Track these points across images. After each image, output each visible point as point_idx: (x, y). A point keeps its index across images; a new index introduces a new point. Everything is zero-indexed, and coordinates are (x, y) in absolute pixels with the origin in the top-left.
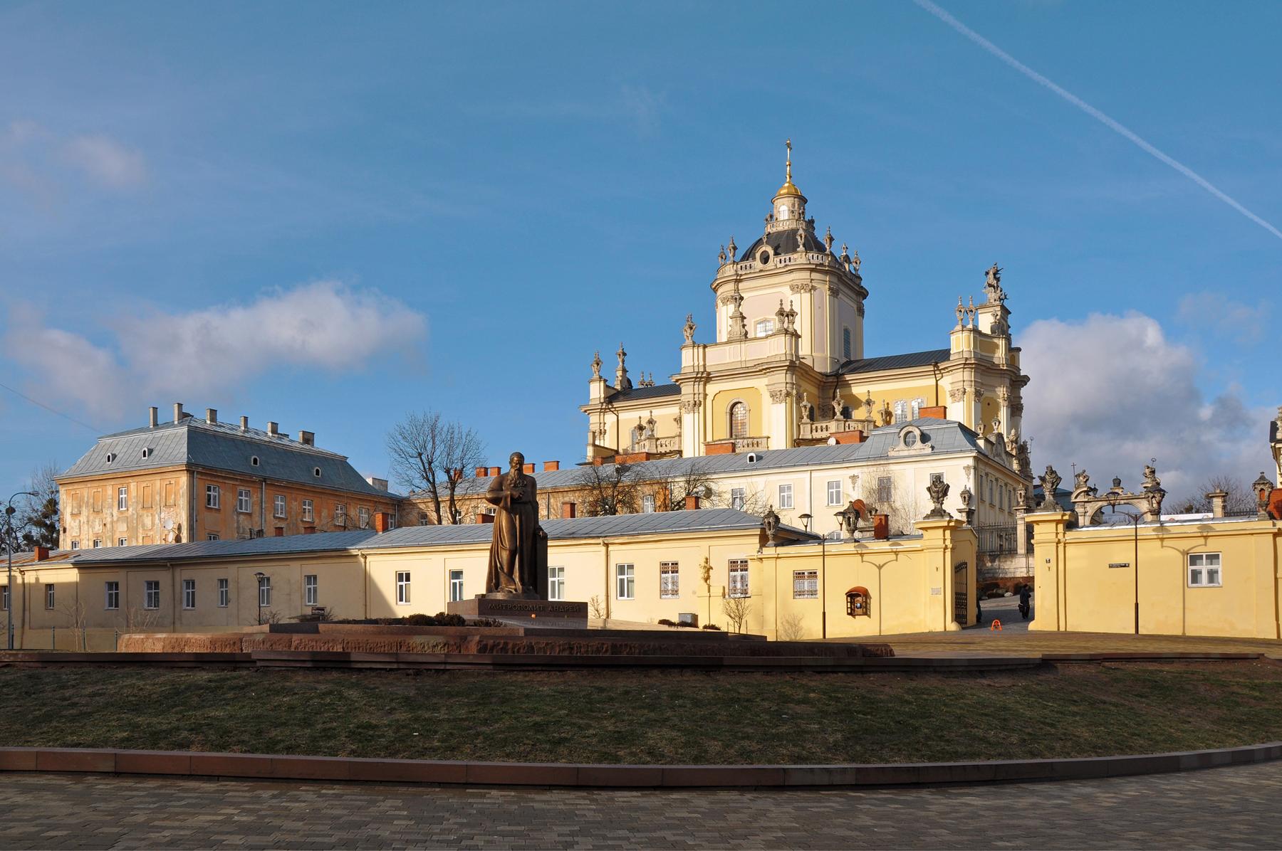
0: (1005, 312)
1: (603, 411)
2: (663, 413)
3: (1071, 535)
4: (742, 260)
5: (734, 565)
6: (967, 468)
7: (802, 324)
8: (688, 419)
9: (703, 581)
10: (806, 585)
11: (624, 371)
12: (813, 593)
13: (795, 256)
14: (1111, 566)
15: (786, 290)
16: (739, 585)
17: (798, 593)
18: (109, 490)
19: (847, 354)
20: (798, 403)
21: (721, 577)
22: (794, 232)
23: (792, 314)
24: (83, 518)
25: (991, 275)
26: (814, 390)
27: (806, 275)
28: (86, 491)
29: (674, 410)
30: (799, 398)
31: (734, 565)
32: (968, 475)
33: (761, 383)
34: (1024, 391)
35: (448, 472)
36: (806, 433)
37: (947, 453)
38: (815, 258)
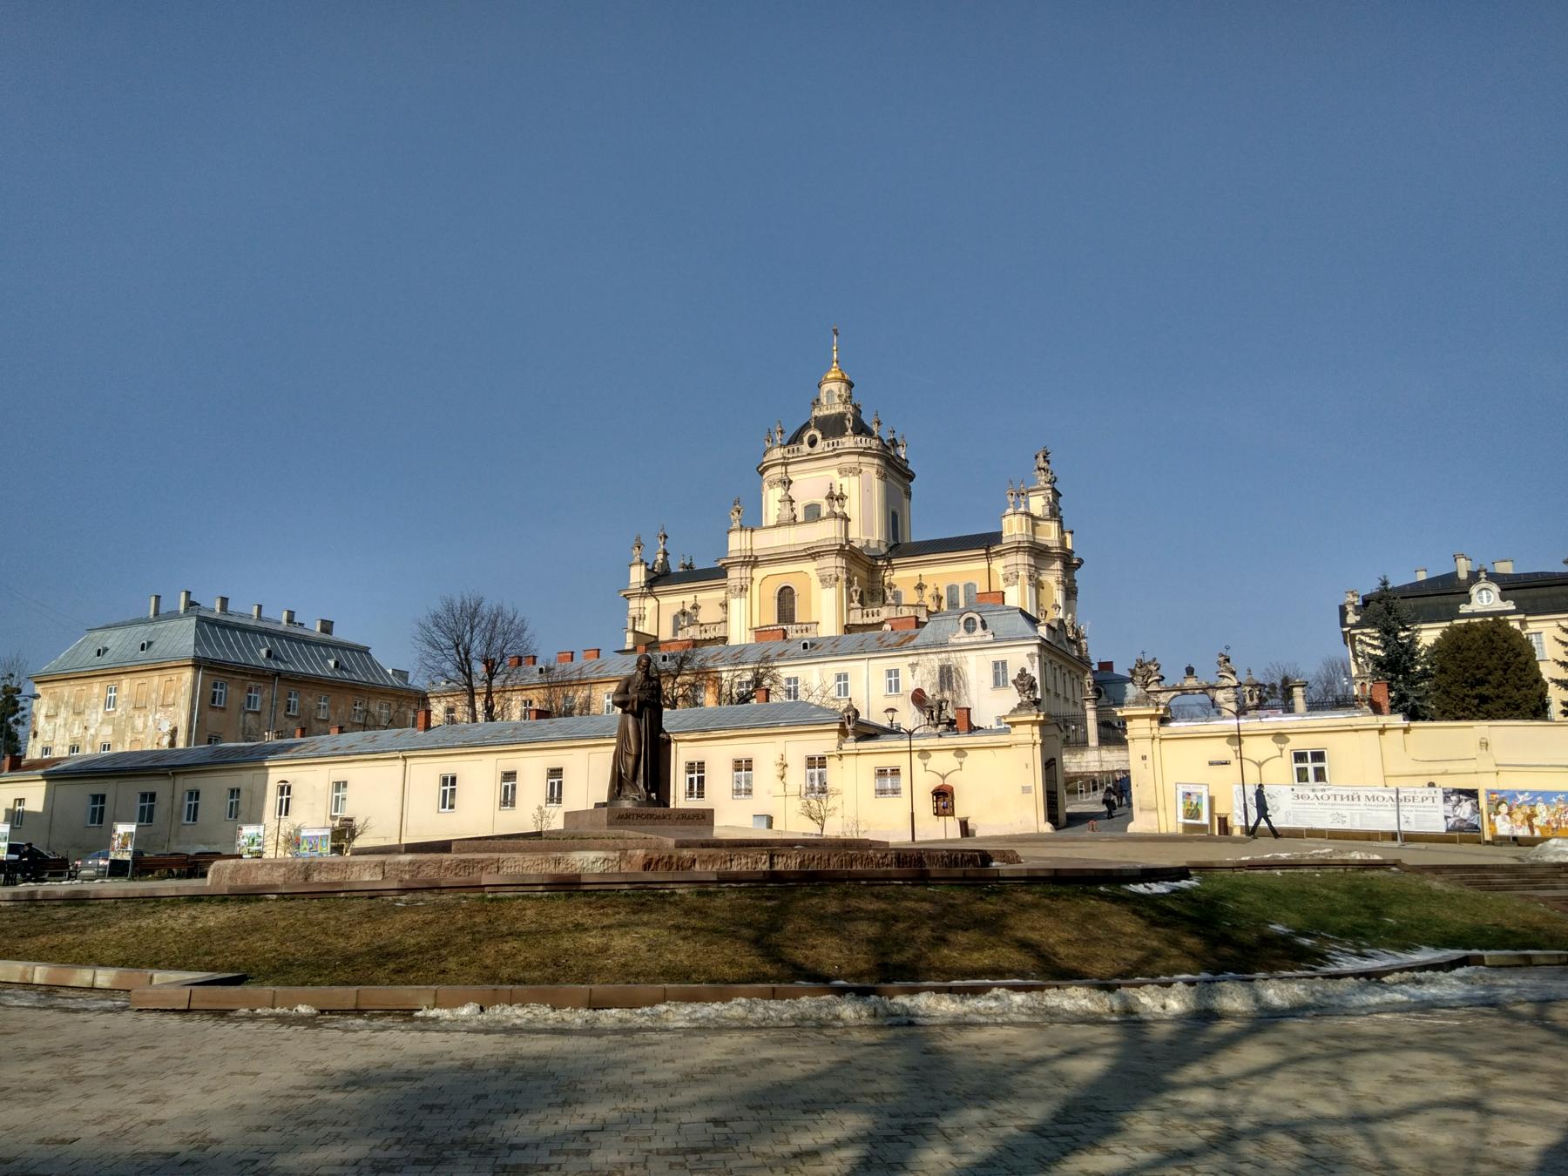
0: (1057, 494)
1: (643, 596)
2: (708, 600)
3: (1164, 730)
4: (789, 443)
5: (811, 762)
6: (1030, 656)
7: (852, 508)
8: (736, 605)
10: (889, 783)
11: (665, 553)
12: (896, 792)
14: (1211, 764)
15: (834, 473)
16: (816, 784)
17: (882, 792)
18: (97, 687)
20: (848, 588)
21: (798, 776)
22: (842, 416)
23: (842, 497)
24: (60, 721)
26: (864, 574)
27: (854, 458)
28: (67, 690)
29: (720, 594)
30: (849, 582)
31: (811, 762)
33: (810, 567)
34: (1077, 574)
35: (486, 662)
36: (857, 618)
37: (1010, 640)
38: (864, 442)
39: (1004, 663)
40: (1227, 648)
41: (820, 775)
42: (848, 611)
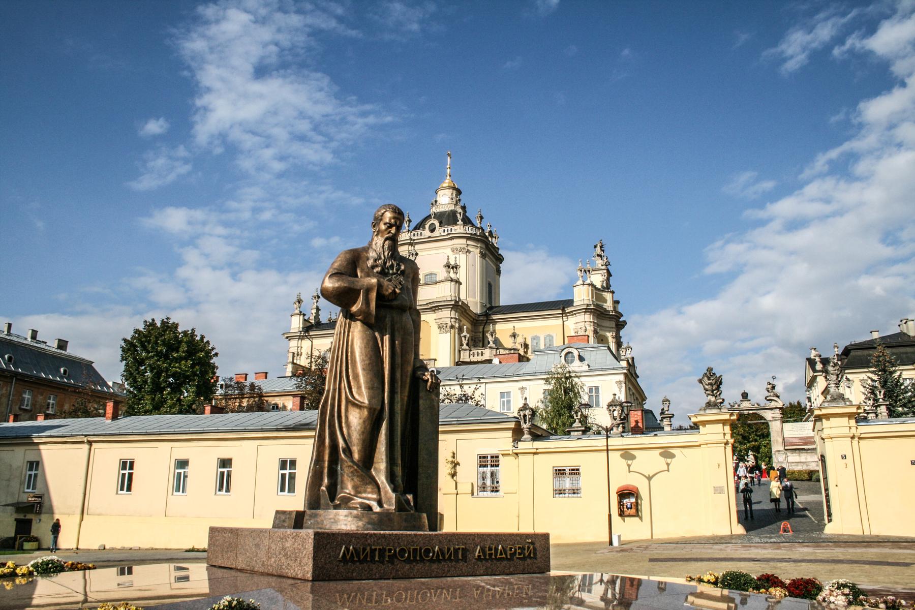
0: (609, 274)
1: (301, 338)
4: (416, 228)
5: (483, 460)
6: (620, 382)
9: (449, 477)
10: (567, 483)
13: (456, 227)
15: (448, 252)
16: (488, 482)
19: (490, 302)
20: (459, 334)
22: (454, 213)
23: (455, 267)
25: (598, 248)
27: (464, 241)
30: (460, 330)
31: (483, 460)
32: (620, 388)
36: (465, 356)
37: (602, 369)
38: (470, 230)
39: (597, 388)
40: (774, 378)
41: (492, 474)
42: (459, 352)
